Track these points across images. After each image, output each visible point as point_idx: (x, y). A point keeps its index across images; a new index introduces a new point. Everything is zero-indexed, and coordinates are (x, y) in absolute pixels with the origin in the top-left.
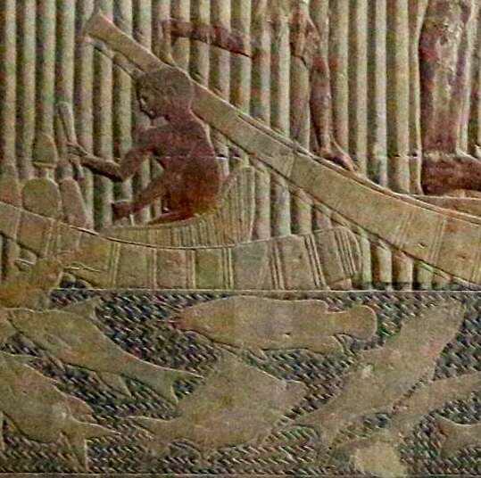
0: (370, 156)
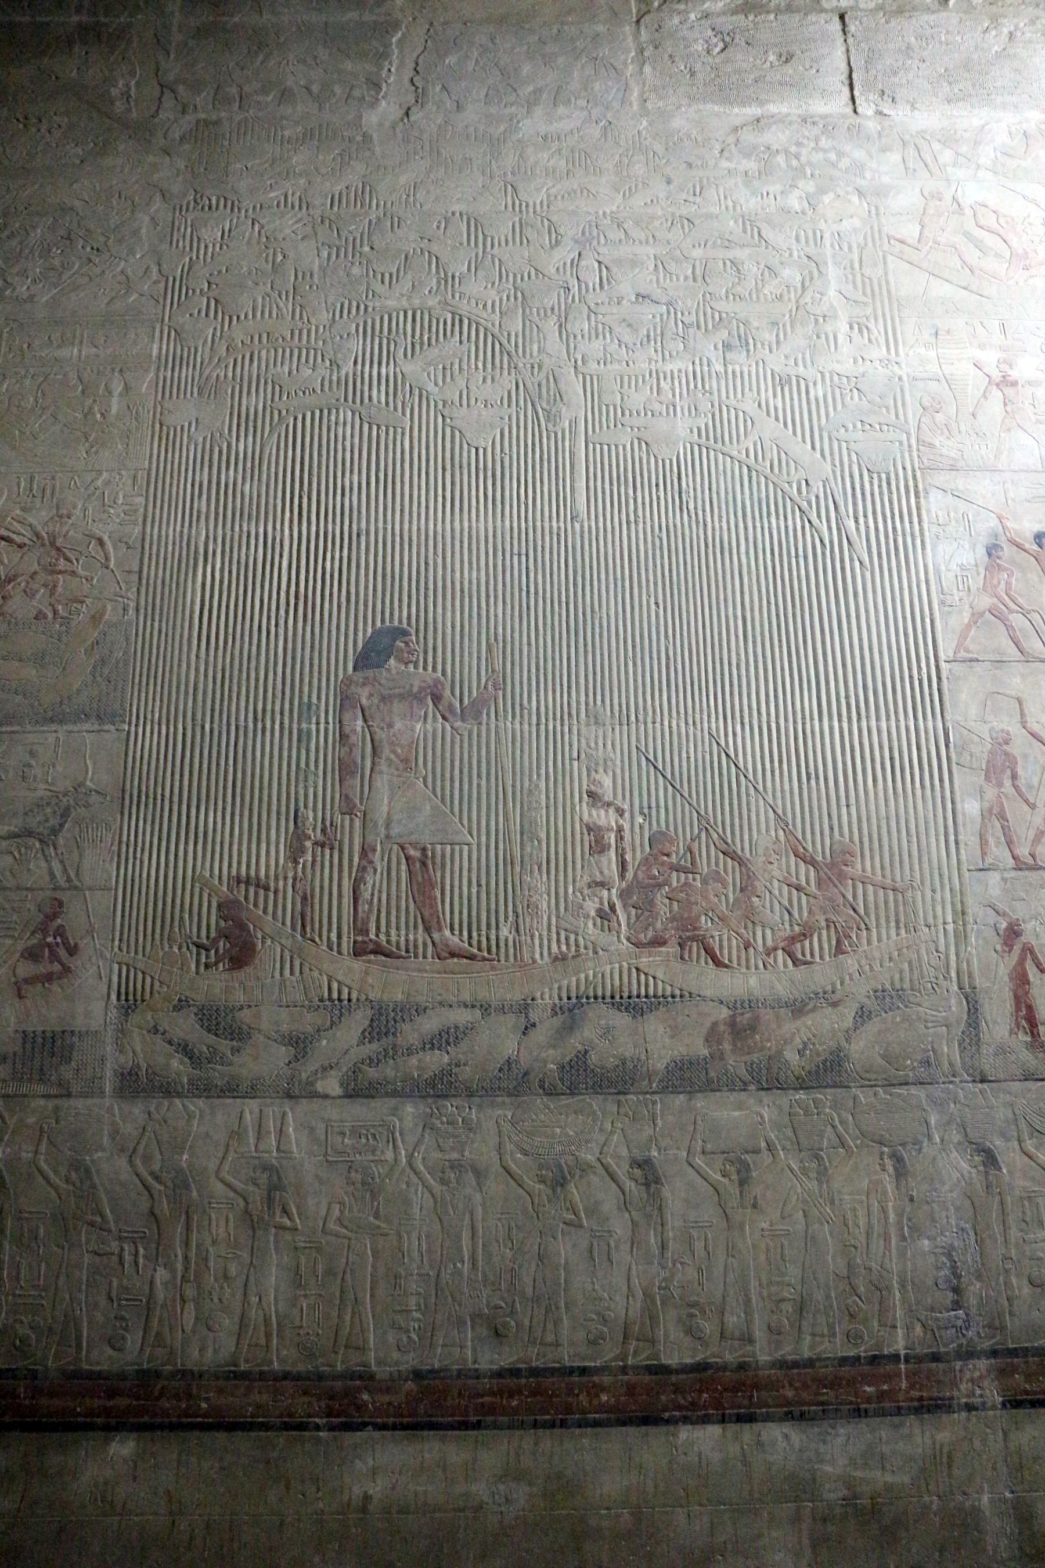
0: (329, 938)
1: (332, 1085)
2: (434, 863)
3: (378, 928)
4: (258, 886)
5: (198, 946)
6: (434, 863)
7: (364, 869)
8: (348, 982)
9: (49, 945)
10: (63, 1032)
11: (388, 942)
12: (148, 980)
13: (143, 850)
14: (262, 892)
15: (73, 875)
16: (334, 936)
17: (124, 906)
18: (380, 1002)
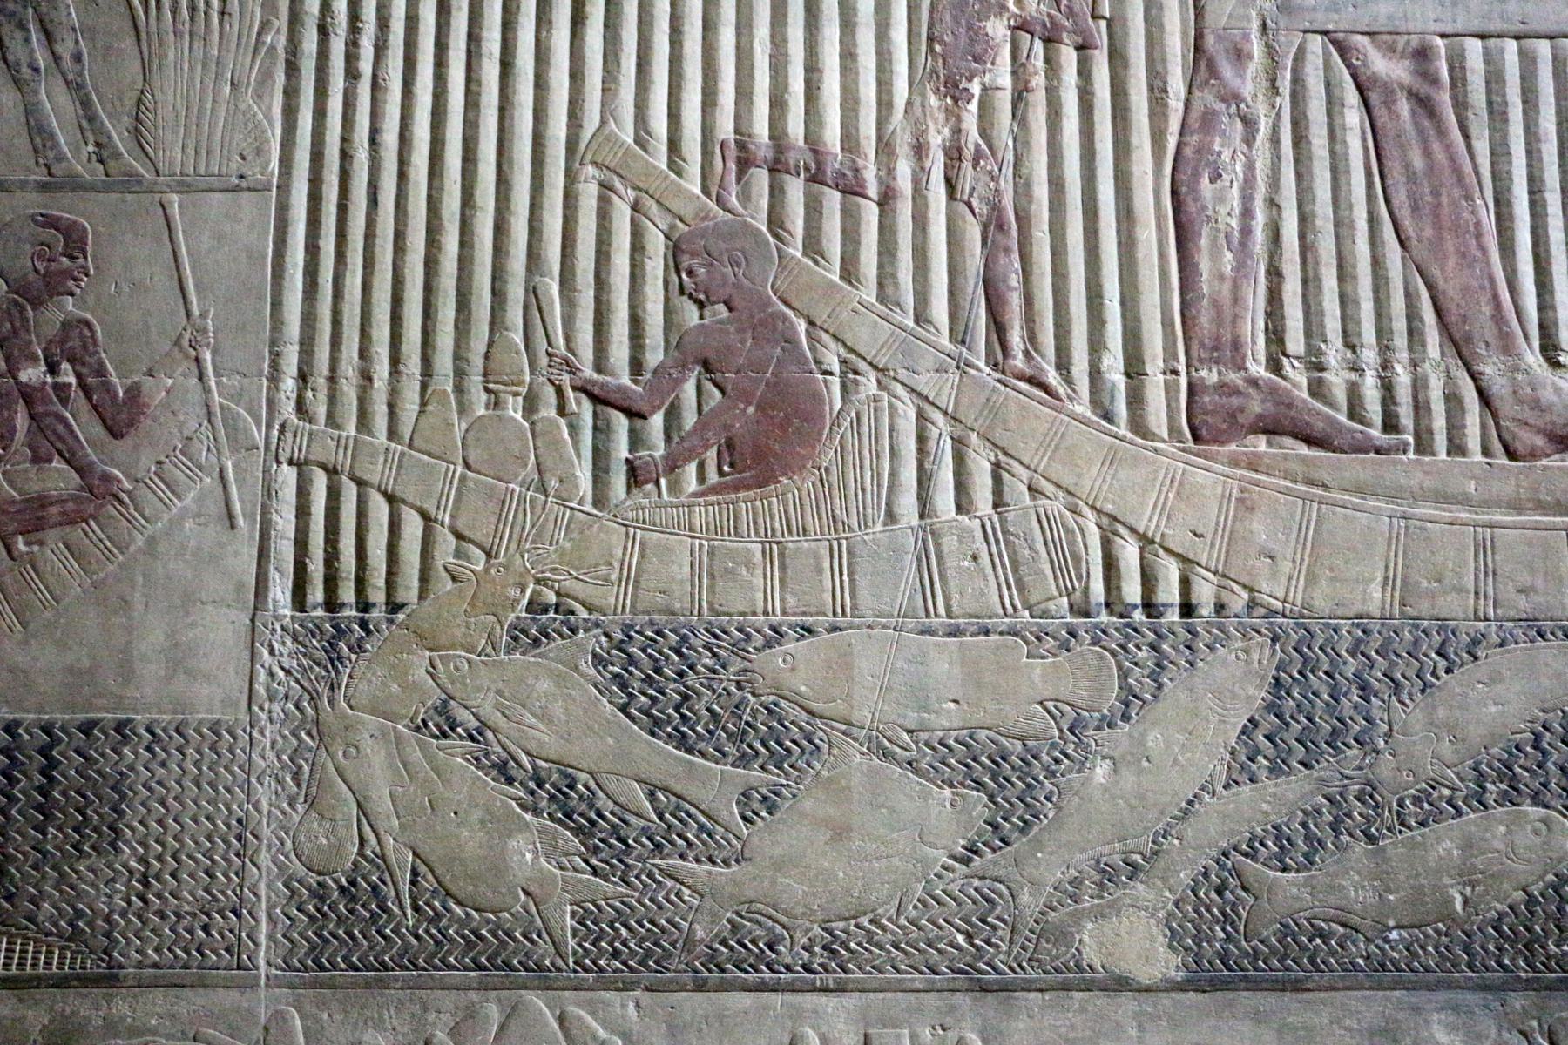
0: (1095, 374)
1: (1135, 939)
2: (1461, 105)
3: (1276, 336)
4: (815, 178)
5: (595, 399)
6: (1461, 105)
7: (1208, 121)
8: (1179, 539)
9: (28, 395)
10: (87, 728)
11: (1318, 389)
12: (413, 527)
13: (380, 49)
14: (833, 199)
15: (119, 139)
16: (1113, 363)
17: (312, 250)
18: (1302, 617)
